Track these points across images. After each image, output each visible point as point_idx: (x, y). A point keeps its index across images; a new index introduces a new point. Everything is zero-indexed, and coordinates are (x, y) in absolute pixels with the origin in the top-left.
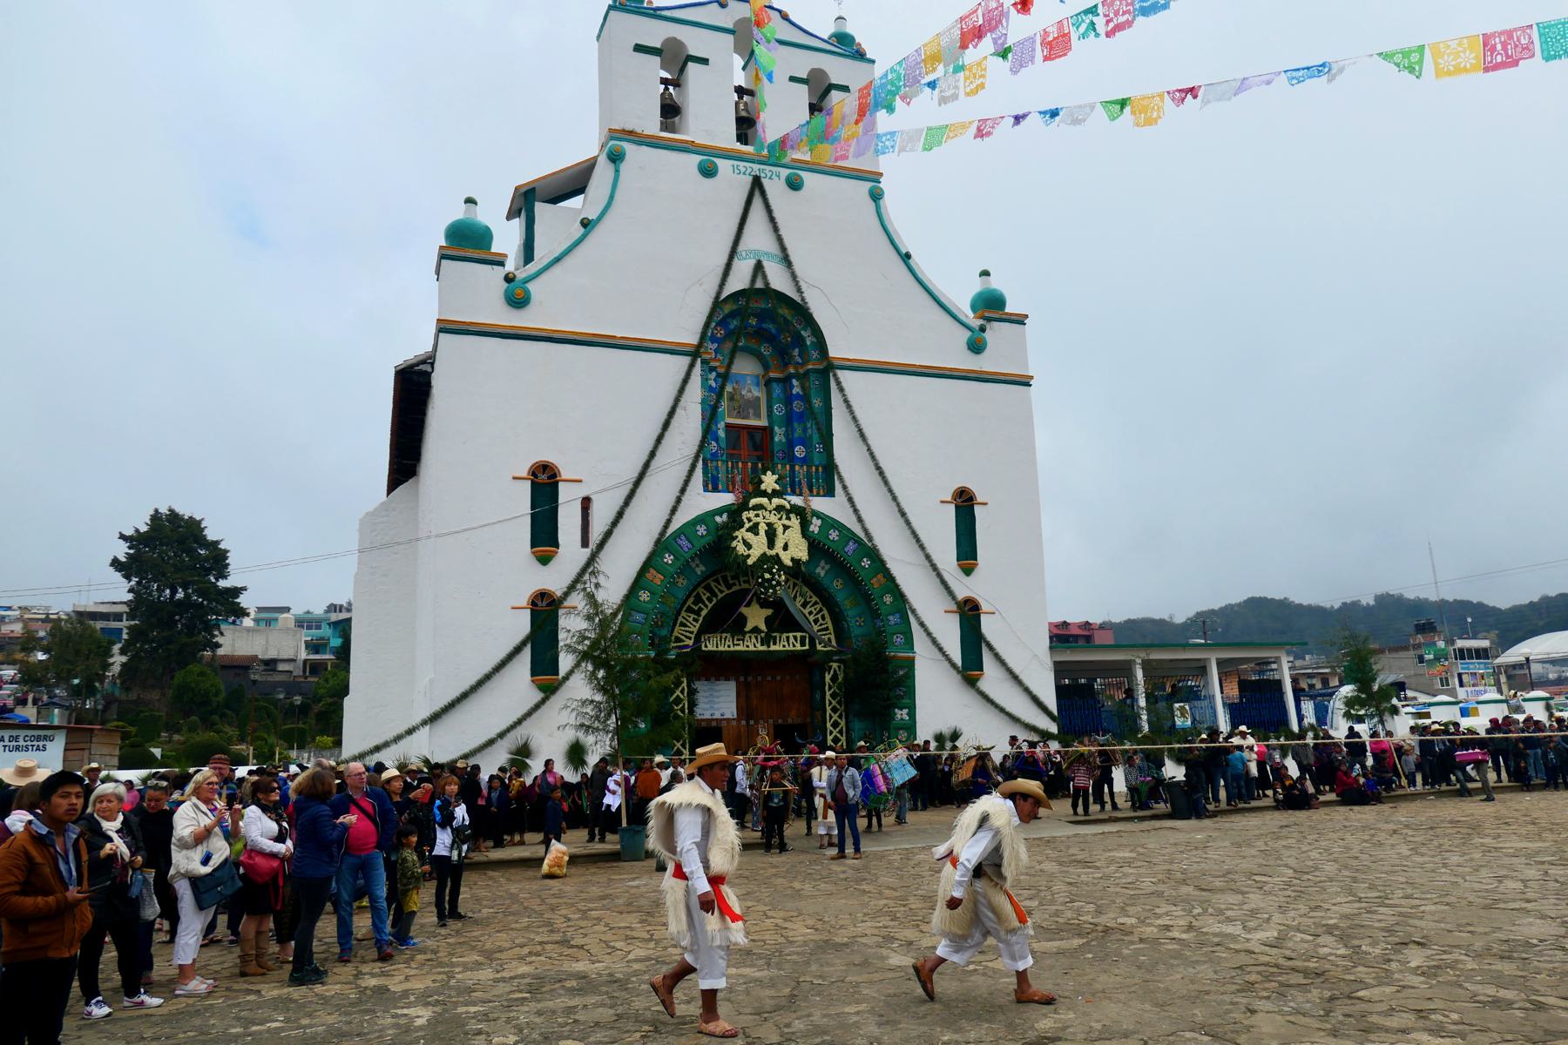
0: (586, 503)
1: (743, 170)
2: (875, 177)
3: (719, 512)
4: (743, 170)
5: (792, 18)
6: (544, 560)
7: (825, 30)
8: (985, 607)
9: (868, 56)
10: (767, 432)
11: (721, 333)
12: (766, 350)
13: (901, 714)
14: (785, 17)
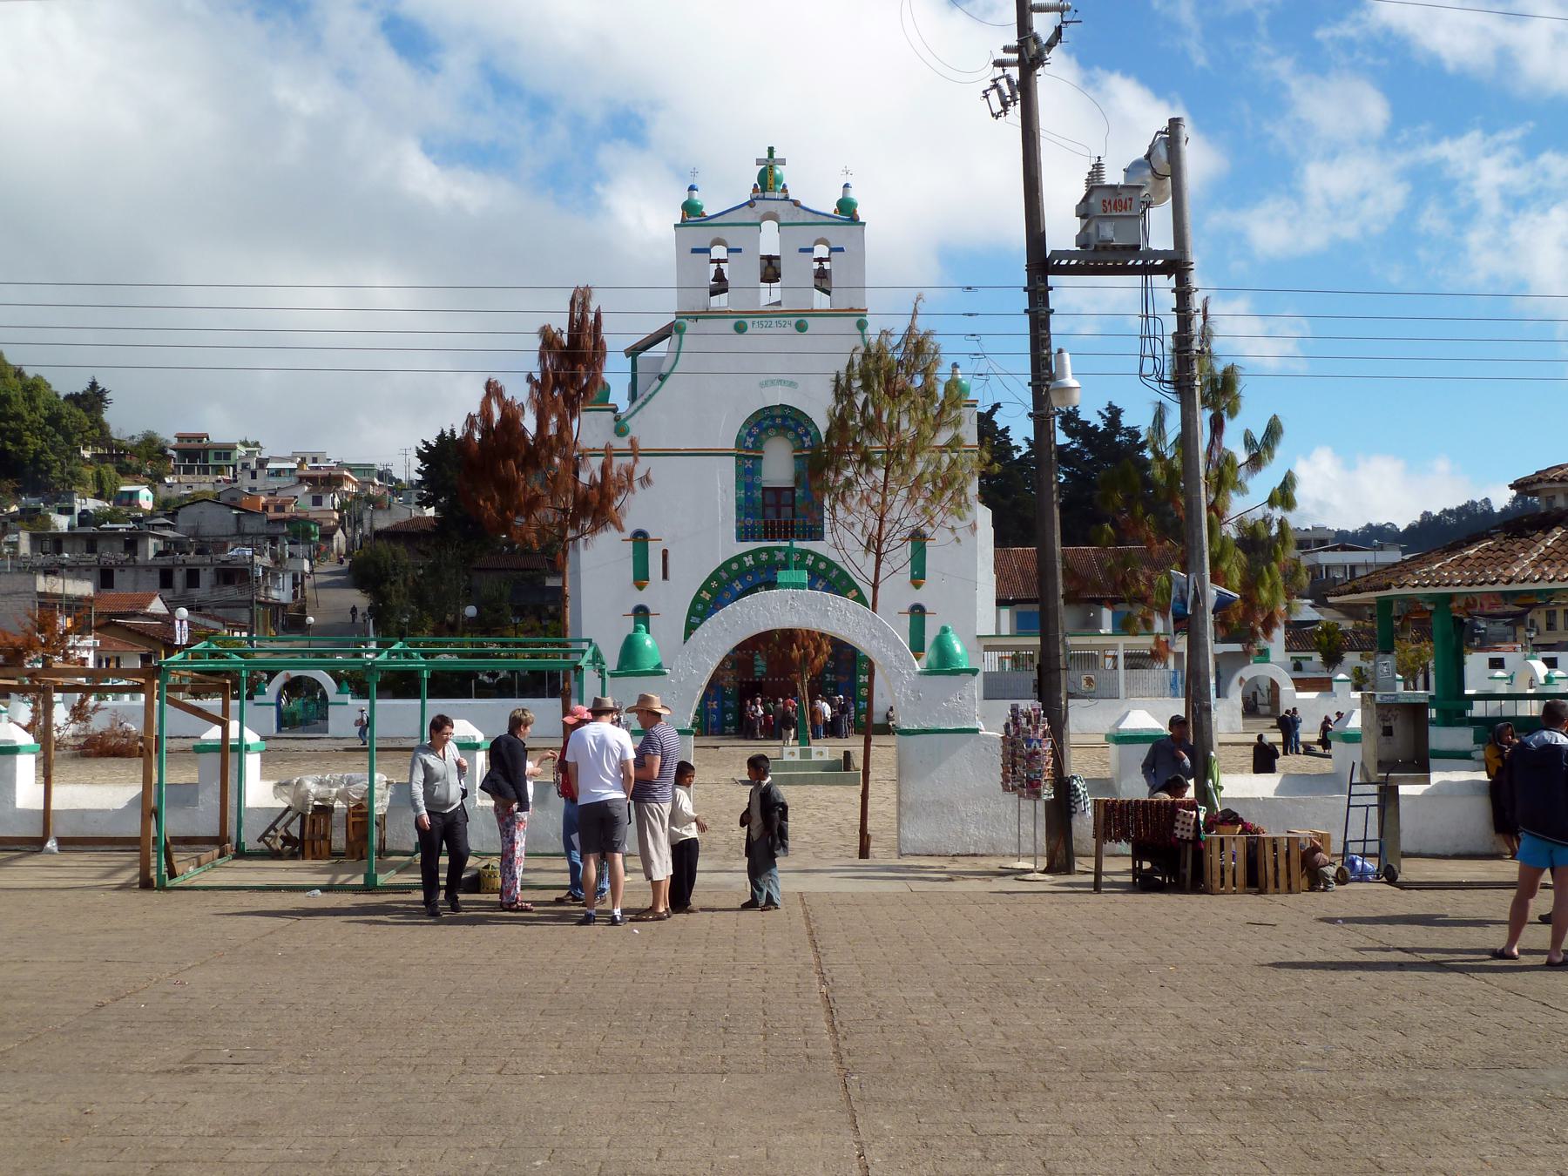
0: (665, 554)
1: (765, 324)
2: (862, 312)
3: (746, 554)
4: (765, 324)
5: (803, 204)
6: (640, 587)
7: (830, 207)
8: (928, 611)
9: (861, 220)
10: (792, 490)
11: (756, 431)
12: (791, 435)
13: (864, 679)
14: (796, 203)
